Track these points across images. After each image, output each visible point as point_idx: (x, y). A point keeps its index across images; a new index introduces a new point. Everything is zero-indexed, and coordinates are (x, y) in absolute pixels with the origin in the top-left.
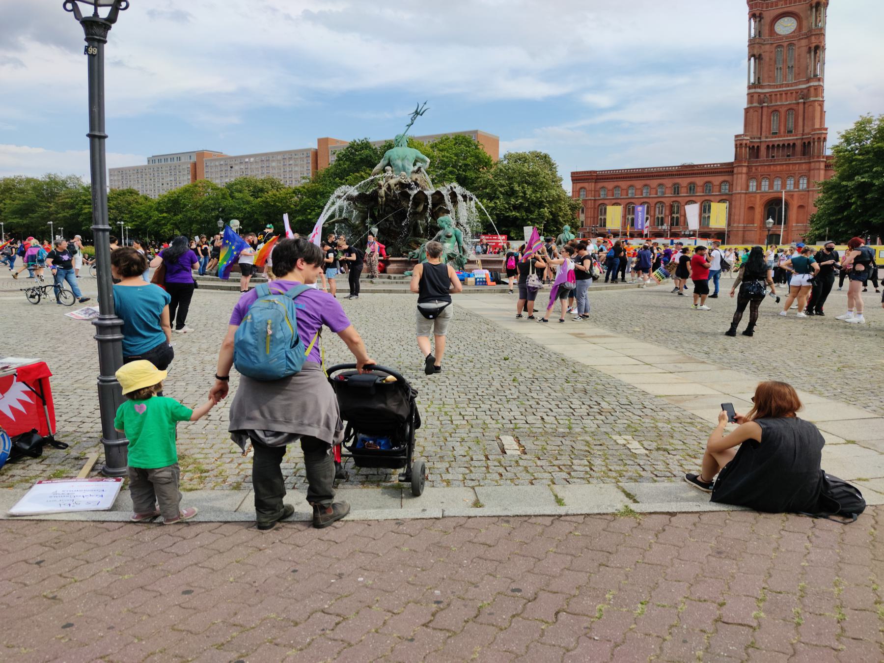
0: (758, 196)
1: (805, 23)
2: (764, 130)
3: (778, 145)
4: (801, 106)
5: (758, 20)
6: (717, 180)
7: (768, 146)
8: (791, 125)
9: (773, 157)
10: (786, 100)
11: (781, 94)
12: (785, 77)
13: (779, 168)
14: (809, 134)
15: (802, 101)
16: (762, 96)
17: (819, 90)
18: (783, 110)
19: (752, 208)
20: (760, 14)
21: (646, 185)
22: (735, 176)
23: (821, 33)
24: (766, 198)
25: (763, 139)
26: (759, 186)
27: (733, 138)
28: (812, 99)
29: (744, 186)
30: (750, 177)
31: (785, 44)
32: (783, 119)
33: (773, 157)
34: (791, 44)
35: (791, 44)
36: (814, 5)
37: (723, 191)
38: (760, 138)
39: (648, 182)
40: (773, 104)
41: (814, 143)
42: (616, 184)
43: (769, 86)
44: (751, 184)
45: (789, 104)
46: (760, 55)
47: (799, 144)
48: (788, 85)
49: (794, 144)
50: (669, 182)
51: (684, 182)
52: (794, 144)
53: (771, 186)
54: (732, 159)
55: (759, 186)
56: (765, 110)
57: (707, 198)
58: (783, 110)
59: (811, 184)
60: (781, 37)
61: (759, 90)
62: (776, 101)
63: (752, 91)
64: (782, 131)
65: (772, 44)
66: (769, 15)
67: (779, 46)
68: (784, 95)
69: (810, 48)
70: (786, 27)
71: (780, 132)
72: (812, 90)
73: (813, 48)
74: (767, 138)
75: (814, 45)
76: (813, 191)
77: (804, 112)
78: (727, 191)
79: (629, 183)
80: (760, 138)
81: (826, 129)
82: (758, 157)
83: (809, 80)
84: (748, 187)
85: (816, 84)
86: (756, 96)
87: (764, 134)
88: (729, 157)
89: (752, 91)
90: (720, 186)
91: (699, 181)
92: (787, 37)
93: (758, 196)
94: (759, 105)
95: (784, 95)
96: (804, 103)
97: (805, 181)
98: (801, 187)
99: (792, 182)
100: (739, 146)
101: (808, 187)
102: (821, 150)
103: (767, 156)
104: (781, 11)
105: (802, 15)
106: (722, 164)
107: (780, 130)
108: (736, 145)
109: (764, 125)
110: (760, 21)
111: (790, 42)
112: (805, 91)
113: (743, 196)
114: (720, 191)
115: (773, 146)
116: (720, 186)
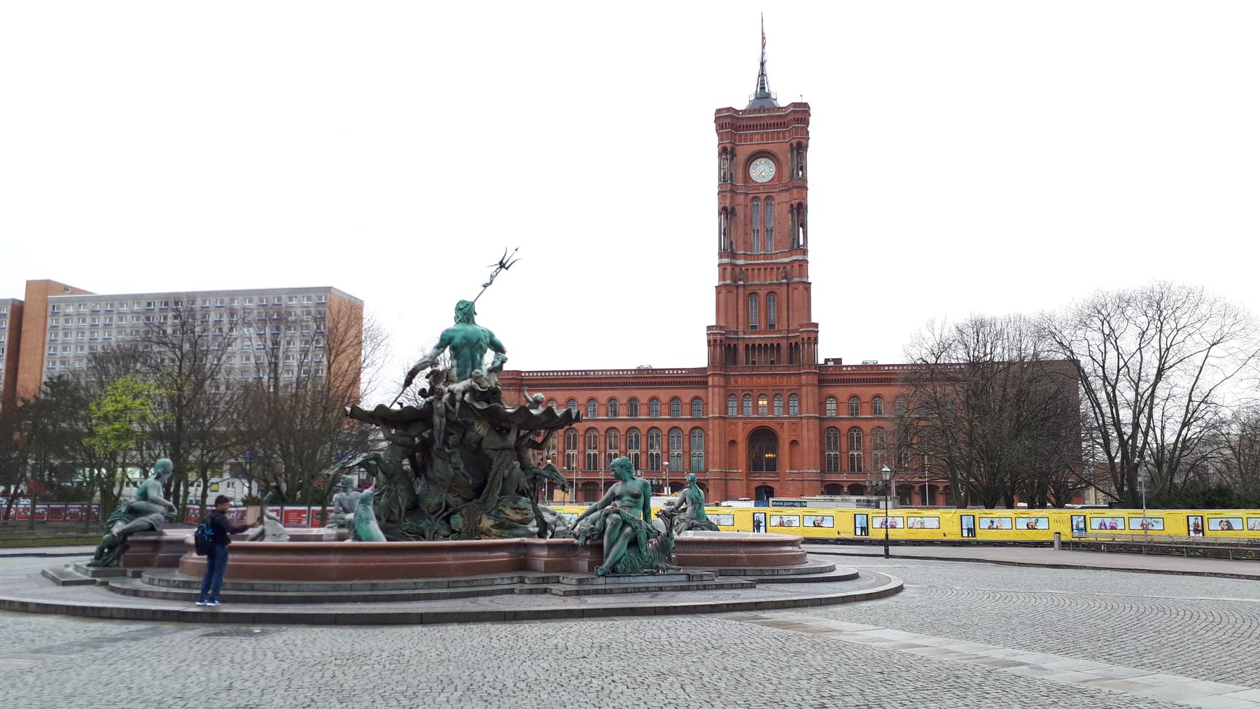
0: (740, 423)
2: (741, 320)
6: (687, 395)
9: (754, 363)
13: (763, 380)
14: (796, 331)
16: (737, 269)
17: (803, 264)
18: (763, 293)
19: (733, 442)
20: (733, 149)
21: (591, 399)
22: (710, 390)
24: (750, 427)
25: (741, 336)
26: (741, 408)
27: (705, 331)
28: (797, 279)
29: (723, 408)
30: (729, 394)
31: (763, 196)
32: (763, 308)
33: (754, 363)
34: (769, 198)
35: (769, 198)
38: (737, 333)
39: (594, 394)
43: (746, 256)
45: (770, 285)
46: (733, 209)
47: (784, 343)
48: (766, 256)
50: (622, 396)
51: (643, 395)
54: (706, 365)
56: (741, 290)
57: (675, 424)
59: (804, 408)
62: (753, 279)
63: (725, 260)
66: (743, 151)
67: (754, 199)
70: (763, 171)
74: (745, 333)
75: (795, 203)
76: (808, 418)
79: (569, 394)
81: (816, 325)
82: (735, 363)
83: (791, 252)
85: (801, 258)
86: (729, 268)
87: (741, 328)
88: (696, 356)
89: (725, 260)
91: (664, 395)
92: (763, 185)
93: (740, 423)
94: (736, 285)
97: (796, 403)
99: (781, 403)
102: (813, 354)
103: (747, 362)
104: (757, 148)
105: (781, 157)
108: (709, 341)
109: (741, 313)
110: (732, 159)
111: (767, 194)
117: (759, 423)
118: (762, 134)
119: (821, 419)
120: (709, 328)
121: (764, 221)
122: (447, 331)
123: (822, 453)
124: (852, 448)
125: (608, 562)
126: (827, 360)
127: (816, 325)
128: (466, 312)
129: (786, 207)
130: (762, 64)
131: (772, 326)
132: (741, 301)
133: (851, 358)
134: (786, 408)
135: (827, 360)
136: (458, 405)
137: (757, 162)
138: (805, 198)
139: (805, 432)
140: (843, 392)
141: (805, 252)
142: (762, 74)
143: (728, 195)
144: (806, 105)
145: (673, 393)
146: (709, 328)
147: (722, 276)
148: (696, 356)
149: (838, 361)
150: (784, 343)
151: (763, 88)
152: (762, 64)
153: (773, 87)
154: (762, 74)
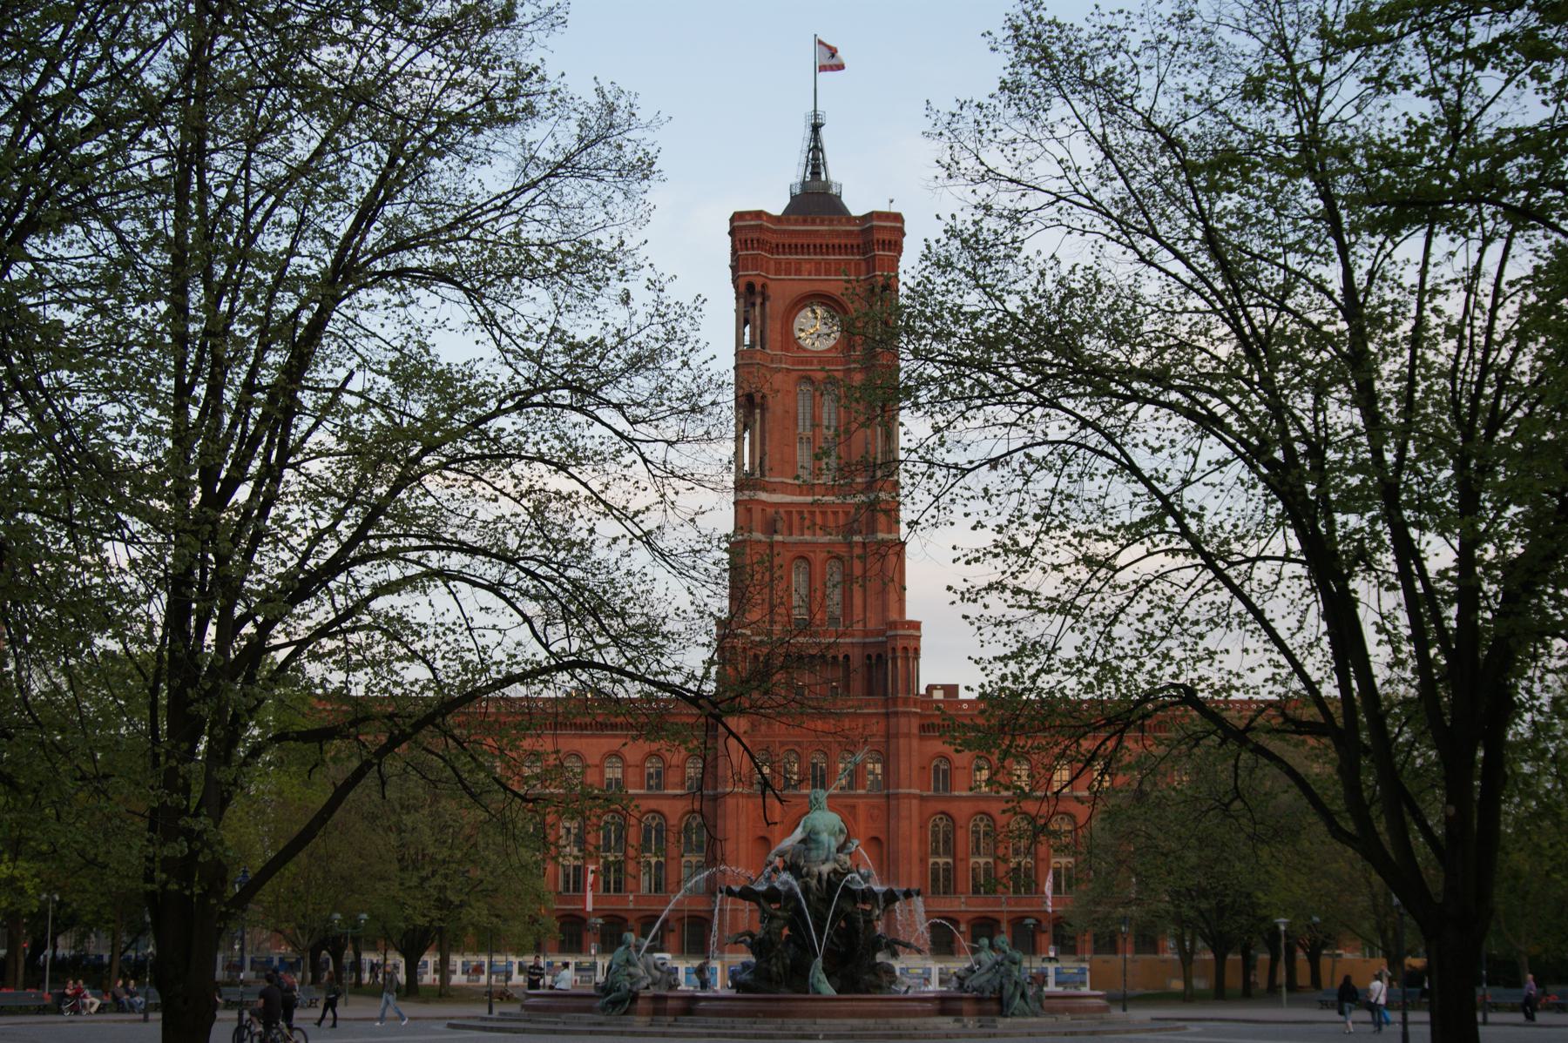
5: (759, 301)
28: (880, 536)
52: (847, 657)
61: (763, 496)
89: (746, 495)
92: (821, 358)
102: (912, 676)
104: (808, 288)
118: (818, 263)
126: (930, 688)
130: (816, 128)
142: (816, 148)
144: (898, 217)
151: (816, 174)
152: (816, 128)
153: (837, 172)
154: (816, 148)
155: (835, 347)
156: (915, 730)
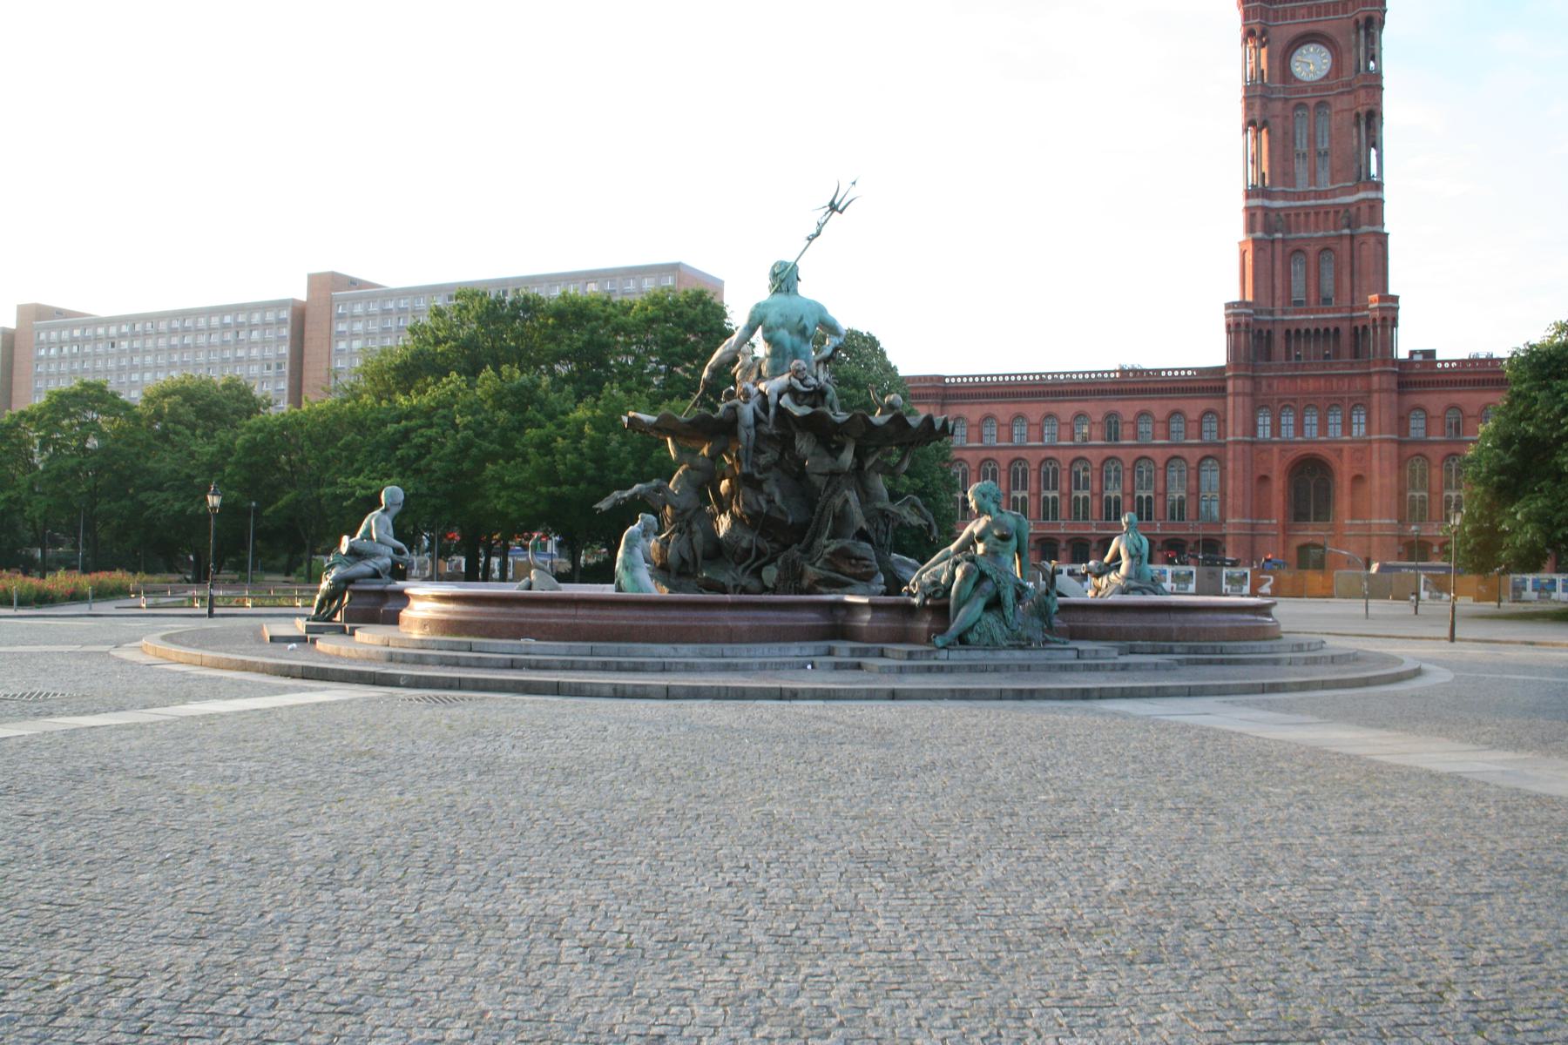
1: (1348, 62)
2: (1279, 292)
3: (1307, 331)
4: (1346, 243)
6: (1194, 407)
7: (1288, 332)
8: (1328, 285)
9: (1298, 357)
10: (1317, 228)
11: (1307, 215)
12: (1314, 175)
13: (1311, 385)
15: (1346, 231)
16: (1272, 215)
17: (1376, 207)
18: (1312, 250)
19: (1264, 479)
21: (1049, 416)
22: (1230, 400)
23: (1374, 85)
24: (1291, 456)
25: (1278, 317)
27: (1222, 311)
28: (1365, 229)
30: (1257, 405)
31: (1312, 103)
34: (1322, 104)
35: (1322, 104)
36: (1362, 22)
37: (1206, 437)
38: (1271, 313)
40: (1293, 235)
41: (1375, 328)
42: (986, 409)
43: (1285, 195)
44: (1260, 421)
45: (1326, 238)
47: (1345, 328)
49: (1337, 330)
50: (1096, 409)
51: (1127, 409)
52: (1337, 330)
53: (1300, 427)
55: (1276, 428)
56: (1279, 247)
57: (1176, 451)
58: (1312, 250)
59: (1375, 426)
60: (1304, 87)
61: (1267, 203)
64: (1312, 298)
65: (1286, 100)
67: (1301, 105)
68: (1312, 217)
69: (1358, 115)
70: (1311, 64)
71: (1308, 302)
72: (1364, 207)
73: (1363, 116)
74: (1284, 313)
75: (1366, 108)
76: (1381, 441)
77: (1352, 257)
78: (1215, 438)
80: (1271, 313)
81: (1395, 299)
84: (1255, 426)
85: (1372, 195)
86: (1259, 214)
87: (1278, 304)
88: (1210, 349)
90: (1200, 422)
91: (1159, 408)
92: (1314, 86)
93: (1276, 449)
95: (1312, 217)
96: (1352, 237)
98: (1355, 433)
99: (1339, 419)
100: (1233, 329)
101: (1369, 432)
102: (1388, 343)
103: (1288, 358)
104: (1302, 29)
106: (1200, 371)
107: (1307, 296)
108: (1228, 326)
109: (1278, 282)
111: (1317, 98)
112: (1353, 210)
113: (1247, 448)
114: (1200, 436)
115: (1298, 331)
116: (1200, 422)
117: (1304, 450)
119: (1400, 443)
120: (1228, 306)
121: (1312, 140)
122: (758, 306)
123: (1401, 494)
124: (1448, 486)
125: (955, 627)
126: (1412, 353)
127: (1395, 299)
128: (784, 279)
129: (1349, 118)
131: (1327, 301)
132: (1278, 265)
133: (1451, 349)
134: (1347, 426)
135: (1412, 353)
136: (772, 411)
137: (1303, 50)
138: (1379, 103)
139: (1375, 462)
140: (1435, 401)
141: (1379, 186)
143: (1258, 103)
145: (1173, 405)
146: (1228, 306)
147: (1250, 228)
148: (1210, 349)
149: (1430, 354)
150: (1345, 328)
155: (1327, 77)
156: (1394, 386)
